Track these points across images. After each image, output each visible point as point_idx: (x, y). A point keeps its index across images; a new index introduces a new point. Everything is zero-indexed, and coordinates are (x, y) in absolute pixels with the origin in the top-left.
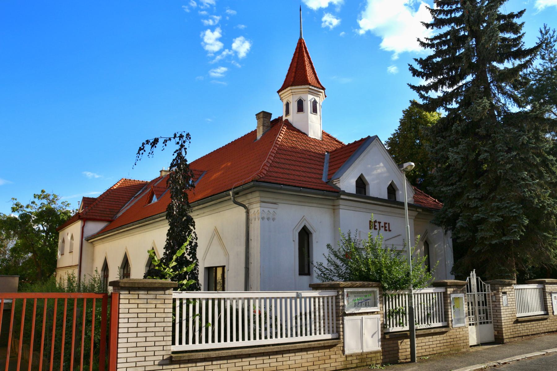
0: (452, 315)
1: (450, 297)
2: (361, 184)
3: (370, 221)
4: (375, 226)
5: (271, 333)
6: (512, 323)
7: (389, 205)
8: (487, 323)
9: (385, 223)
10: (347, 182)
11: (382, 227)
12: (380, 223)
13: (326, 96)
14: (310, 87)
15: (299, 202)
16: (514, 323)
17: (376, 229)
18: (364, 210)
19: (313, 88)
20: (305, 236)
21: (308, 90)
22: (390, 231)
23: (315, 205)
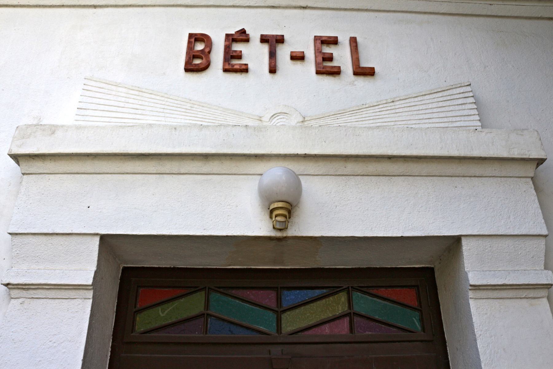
3: (194, 38)
11: (298, 57)
12: (273, 42)
22: (364, 72)
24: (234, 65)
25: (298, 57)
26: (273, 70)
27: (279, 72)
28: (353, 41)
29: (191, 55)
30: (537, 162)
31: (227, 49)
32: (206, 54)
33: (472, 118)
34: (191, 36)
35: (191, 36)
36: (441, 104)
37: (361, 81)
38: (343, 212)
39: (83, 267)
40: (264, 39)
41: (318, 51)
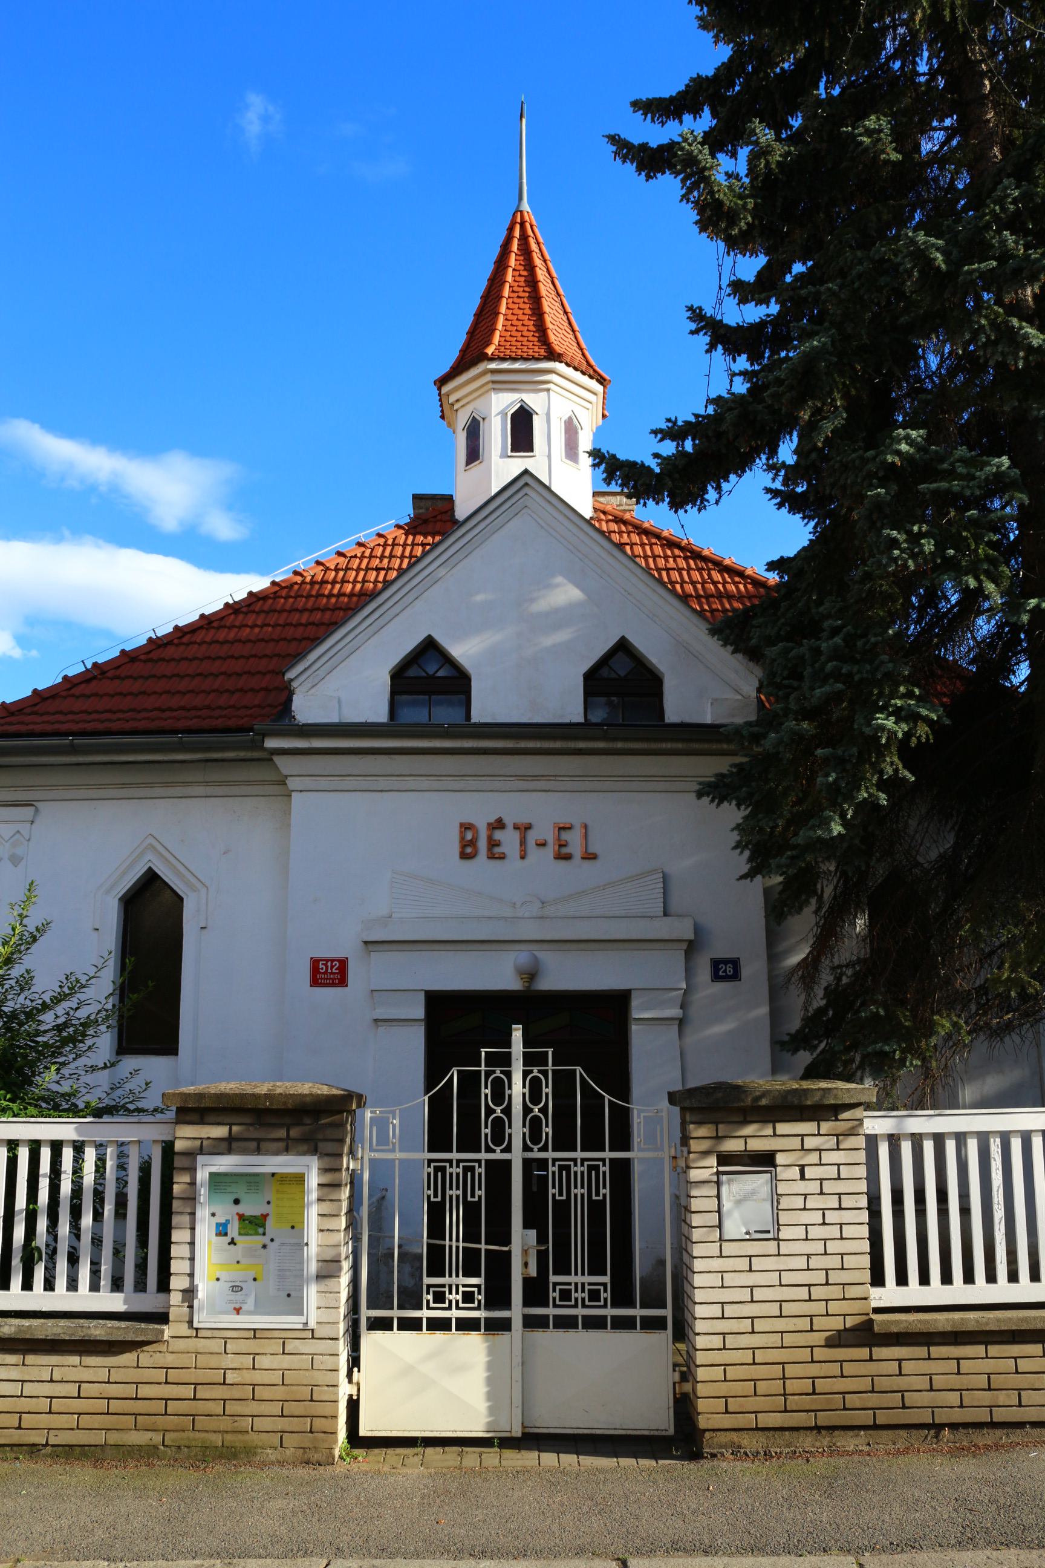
0: (205, 1256)
1: (192, 1170)
2: (429, 680)
3: (466, 827)
4: (493, 844)
5: (141, 1267)
6: (819, 1338)
7: (558, 745)
8: (624, 1324)
10: (346, 682)
11: (542, 844)
12: (524, 829)
13: (601, 381)
14: (493, 366)
15: (124, 785)
16: (830, 1343)
17: (502, 857)
18: (425, 783)
19: (505, 365)
21: (489, 377)
23: (200, 790)
24: (494, 852)
25: (542, 844)
26: (523, 858)
27: (526, 861)
30: (685, 946)
31: (490, 838)
32: (473, 843)
34: (461, 825)
35: (461, 825)
38: (565, 975)
39: (420, 1012)
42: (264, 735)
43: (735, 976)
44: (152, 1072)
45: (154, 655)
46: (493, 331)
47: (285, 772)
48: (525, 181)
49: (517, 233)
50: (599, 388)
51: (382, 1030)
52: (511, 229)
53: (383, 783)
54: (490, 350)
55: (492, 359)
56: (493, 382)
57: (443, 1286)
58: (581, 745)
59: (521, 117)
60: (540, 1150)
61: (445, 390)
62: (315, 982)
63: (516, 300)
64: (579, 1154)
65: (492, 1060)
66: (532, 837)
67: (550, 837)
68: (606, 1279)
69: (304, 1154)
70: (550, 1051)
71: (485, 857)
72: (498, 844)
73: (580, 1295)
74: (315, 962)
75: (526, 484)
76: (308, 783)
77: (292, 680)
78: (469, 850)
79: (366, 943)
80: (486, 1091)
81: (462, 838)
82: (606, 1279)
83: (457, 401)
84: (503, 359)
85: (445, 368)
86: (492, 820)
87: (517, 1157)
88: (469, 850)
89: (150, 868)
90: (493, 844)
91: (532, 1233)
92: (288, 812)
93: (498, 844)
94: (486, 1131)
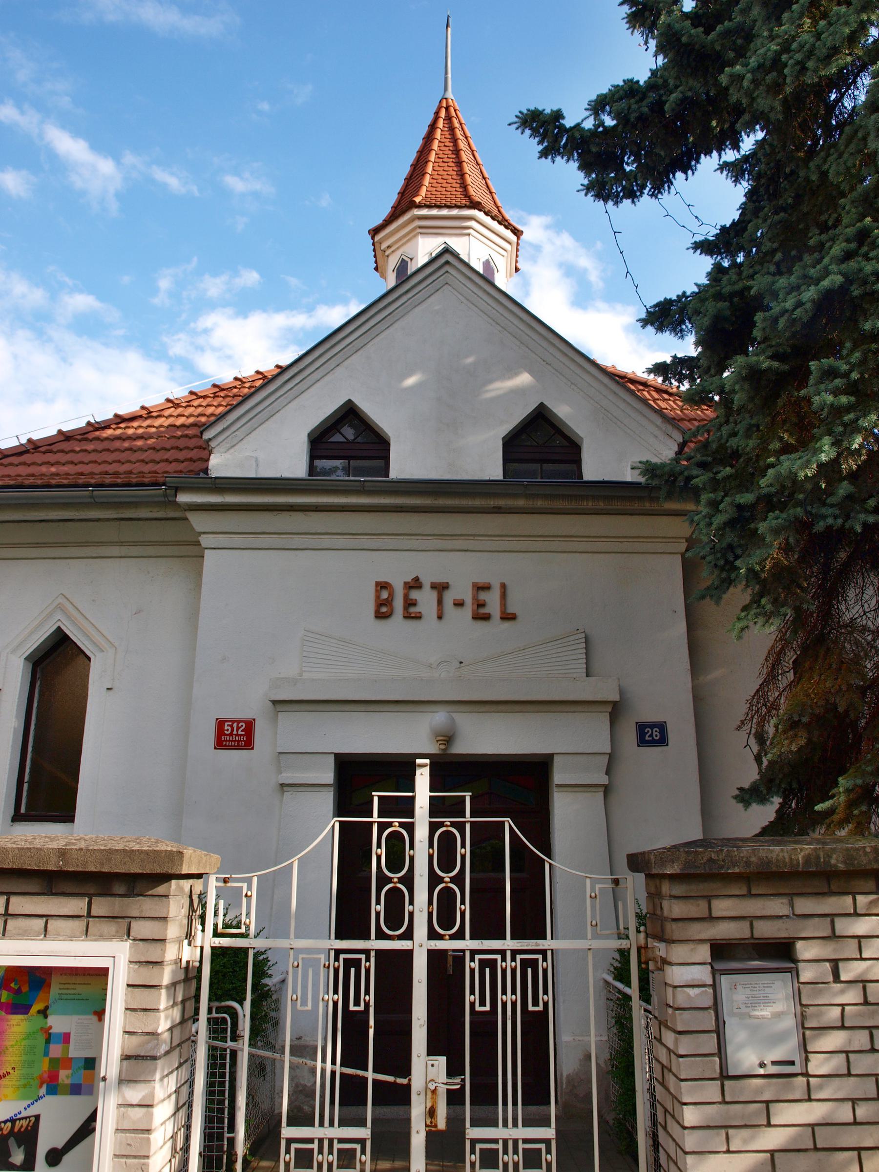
2: (349, 442)
4: (409, 603)
9: (481, 588)
11: (459, 604)
12: (441, 588)
17: (418, 617)
18: (341, 541)
20: (57, 665)
22: (508, 617)
24: (411, 613)
25: (459, 604)
26: (440, 617)
27: (444, 620)
28: (503, 586)
29: (380, 604)
31: (406, 596)
32: (388, 602)
33: (580, 661)
34: (377, 584)
35: (377, 584)
36: (559, 650)
37: (507, 625)
39: (328, 776)
40: (434, 586)
41: (475, 598)
42: (177, 490)
43: (663, 741)
44: (44, 838)
45: (91, 436)
46: (421, 185)
47: (198, 529)
48: (449, 75)
49: (443, 114)
50: (514, 238)
51: (287, 795)
52: (437, 113)
53: (297, 541)
54: (418, 200)
55: (419, 206)
56: (420, 227)
57: (311, 1141)
58: (501, 502)
59: (447, 26)
60: (453, 937)
61: (377, 238)
62: (220, 744)
63: (441, 164)
64: (509, 944)
65: (389, 808)
66: (449, 598)
67: (468, 597)
68: (549, 1133)
69: (110, 938)
70: (468, 795)
71: (401, 617)
72: (414, 604)
73: (510, 1158)
74: (220, 723)
75: (447, 263)
76: (222, 540)
77: (210, 439)
78: (384, 609)
79: (275, 702)
80: (379, 852)
81: (378, 597)
82: (549, 1133)
83: (389, 247)
84: (429, 207)
85: (379, 221)
86: (409, 579)
87: (421, 946)
88: (384, 609)
89: (59, 627)
90: (409, 603)
91: (442, 1061)
92: (200, 573)
93: (414, 604)
94: (377, 908)
